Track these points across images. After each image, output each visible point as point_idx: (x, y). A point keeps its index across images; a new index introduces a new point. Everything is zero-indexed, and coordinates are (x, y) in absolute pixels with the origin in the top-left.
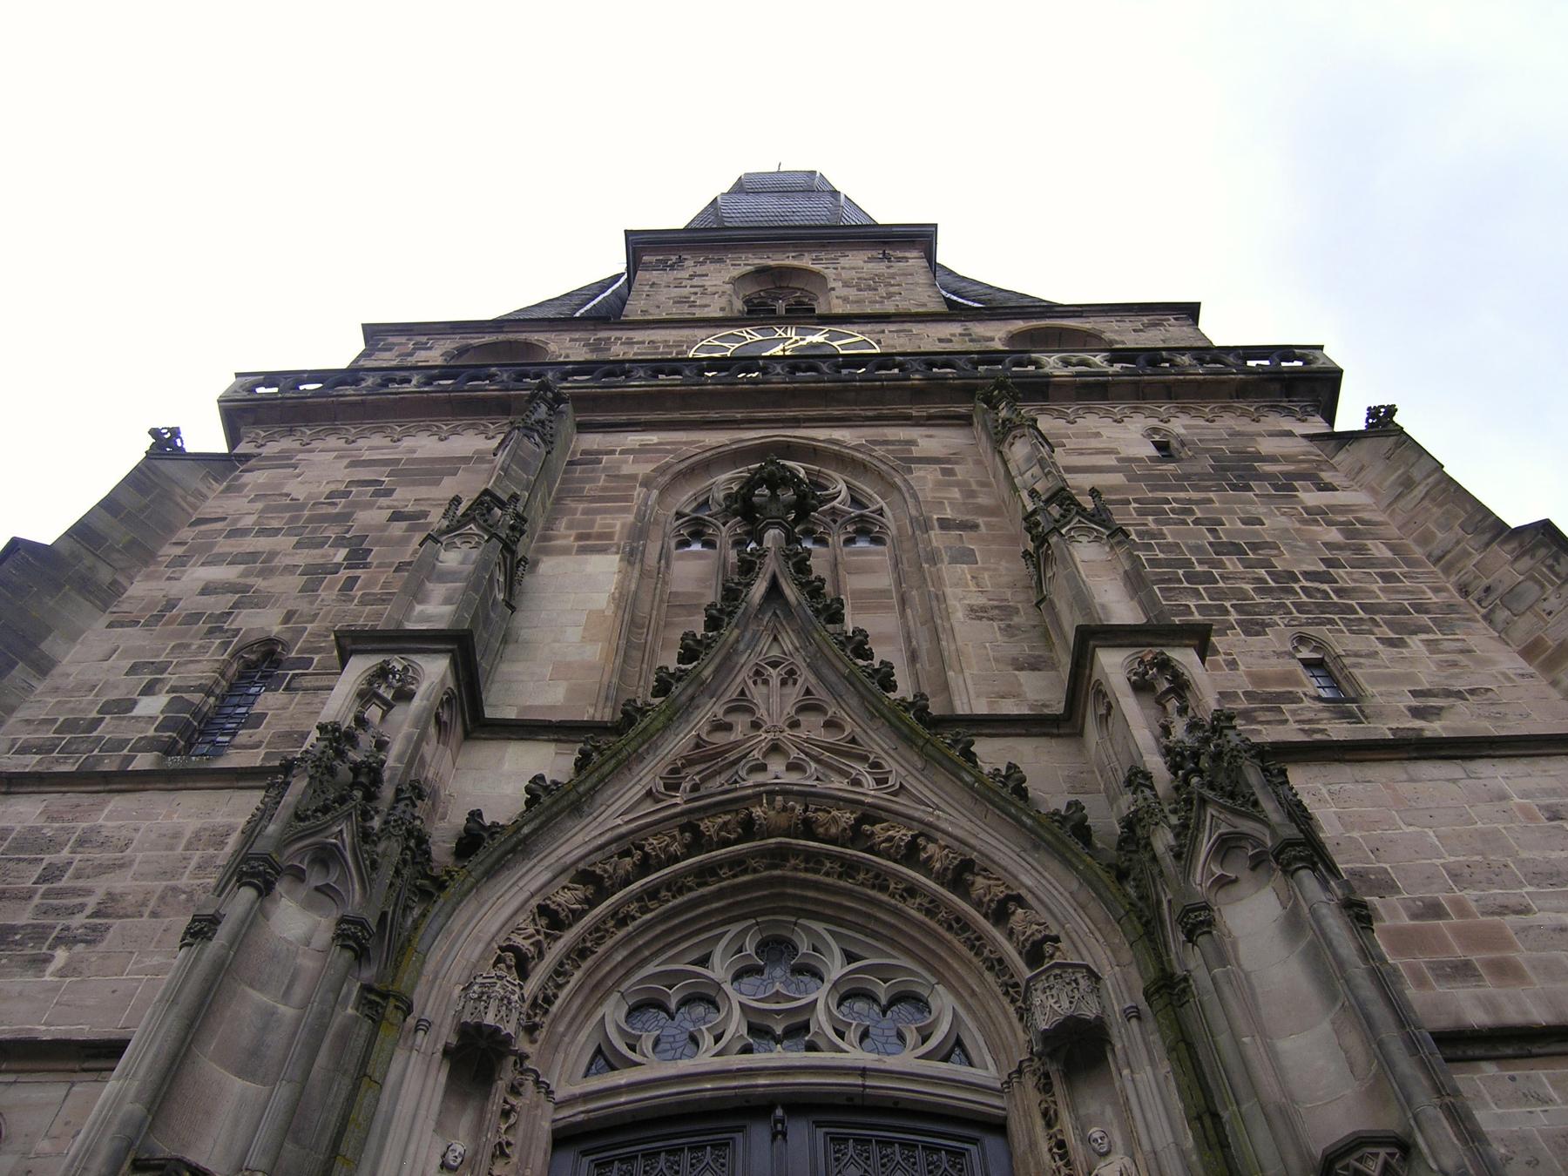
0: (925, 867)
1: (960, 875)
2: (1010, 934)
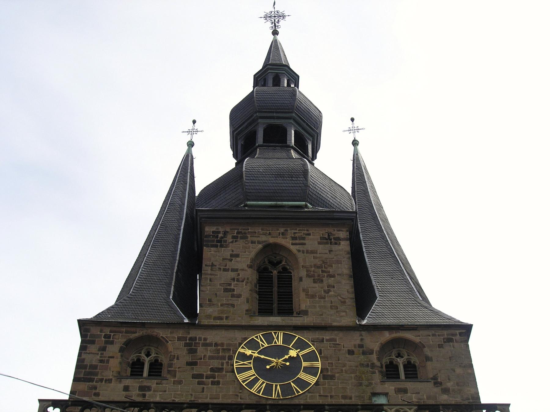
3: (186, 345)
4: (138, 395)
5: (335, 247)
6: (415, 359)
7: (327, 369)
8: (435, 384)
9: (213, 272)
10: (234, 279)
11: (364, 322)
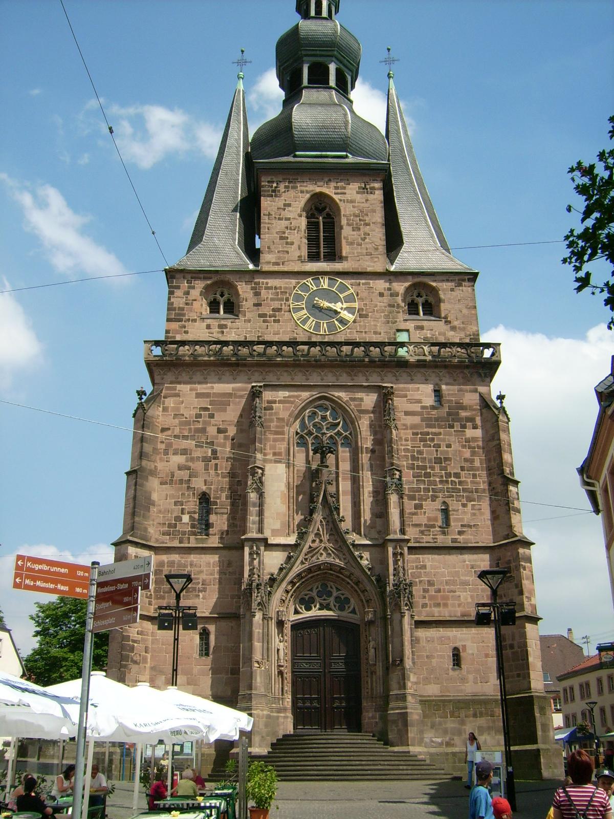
0: (352, 580)
1: (357, 583)
2: (364, 596)
3: (252, 289)
4: (218, 332)
5: (371, 197)
6: (431, 300)
7: (363, 309)
8: (446, 322)
9: (270, 221)
10: (287, 228)
11: (392, 269)
